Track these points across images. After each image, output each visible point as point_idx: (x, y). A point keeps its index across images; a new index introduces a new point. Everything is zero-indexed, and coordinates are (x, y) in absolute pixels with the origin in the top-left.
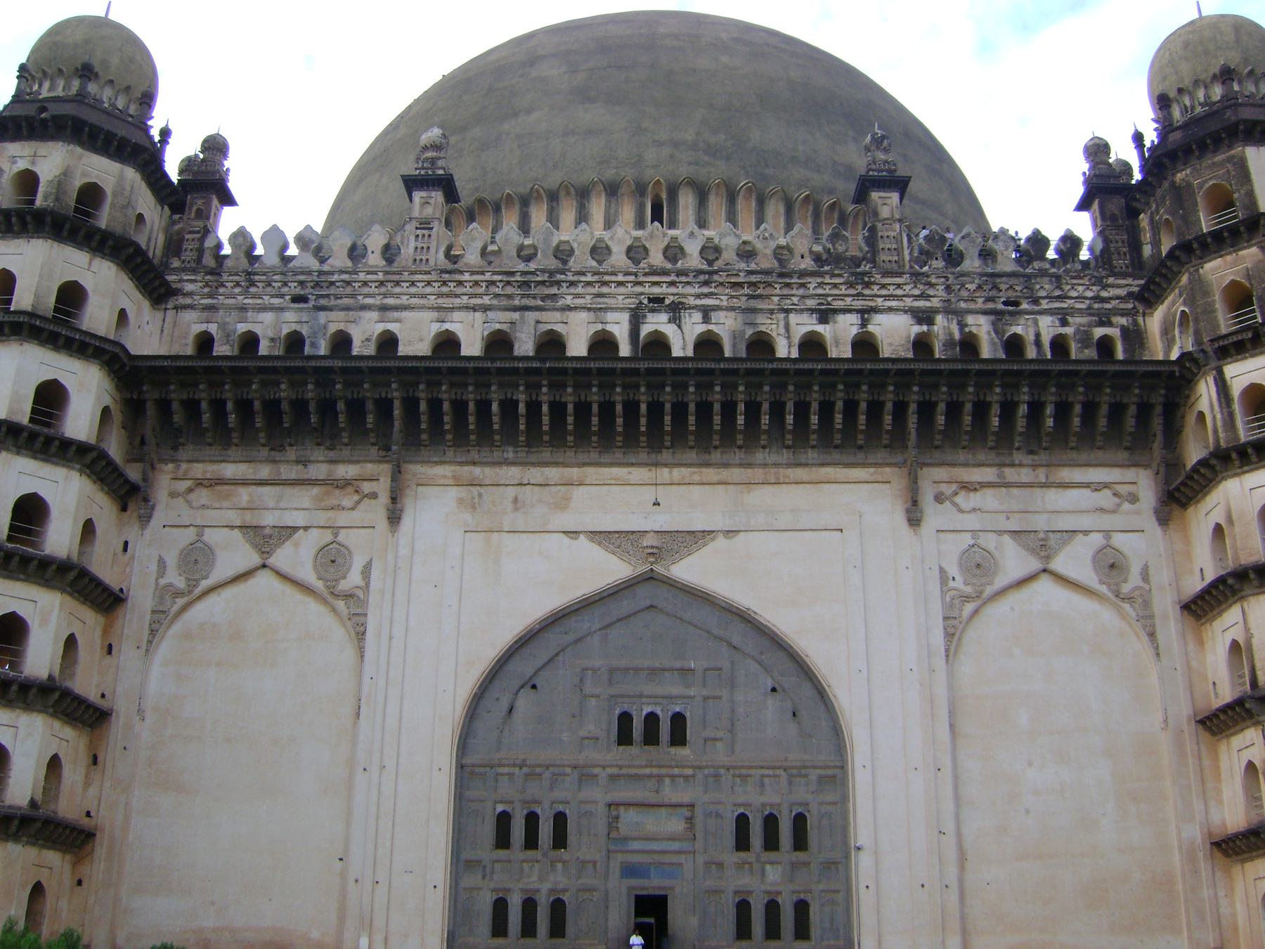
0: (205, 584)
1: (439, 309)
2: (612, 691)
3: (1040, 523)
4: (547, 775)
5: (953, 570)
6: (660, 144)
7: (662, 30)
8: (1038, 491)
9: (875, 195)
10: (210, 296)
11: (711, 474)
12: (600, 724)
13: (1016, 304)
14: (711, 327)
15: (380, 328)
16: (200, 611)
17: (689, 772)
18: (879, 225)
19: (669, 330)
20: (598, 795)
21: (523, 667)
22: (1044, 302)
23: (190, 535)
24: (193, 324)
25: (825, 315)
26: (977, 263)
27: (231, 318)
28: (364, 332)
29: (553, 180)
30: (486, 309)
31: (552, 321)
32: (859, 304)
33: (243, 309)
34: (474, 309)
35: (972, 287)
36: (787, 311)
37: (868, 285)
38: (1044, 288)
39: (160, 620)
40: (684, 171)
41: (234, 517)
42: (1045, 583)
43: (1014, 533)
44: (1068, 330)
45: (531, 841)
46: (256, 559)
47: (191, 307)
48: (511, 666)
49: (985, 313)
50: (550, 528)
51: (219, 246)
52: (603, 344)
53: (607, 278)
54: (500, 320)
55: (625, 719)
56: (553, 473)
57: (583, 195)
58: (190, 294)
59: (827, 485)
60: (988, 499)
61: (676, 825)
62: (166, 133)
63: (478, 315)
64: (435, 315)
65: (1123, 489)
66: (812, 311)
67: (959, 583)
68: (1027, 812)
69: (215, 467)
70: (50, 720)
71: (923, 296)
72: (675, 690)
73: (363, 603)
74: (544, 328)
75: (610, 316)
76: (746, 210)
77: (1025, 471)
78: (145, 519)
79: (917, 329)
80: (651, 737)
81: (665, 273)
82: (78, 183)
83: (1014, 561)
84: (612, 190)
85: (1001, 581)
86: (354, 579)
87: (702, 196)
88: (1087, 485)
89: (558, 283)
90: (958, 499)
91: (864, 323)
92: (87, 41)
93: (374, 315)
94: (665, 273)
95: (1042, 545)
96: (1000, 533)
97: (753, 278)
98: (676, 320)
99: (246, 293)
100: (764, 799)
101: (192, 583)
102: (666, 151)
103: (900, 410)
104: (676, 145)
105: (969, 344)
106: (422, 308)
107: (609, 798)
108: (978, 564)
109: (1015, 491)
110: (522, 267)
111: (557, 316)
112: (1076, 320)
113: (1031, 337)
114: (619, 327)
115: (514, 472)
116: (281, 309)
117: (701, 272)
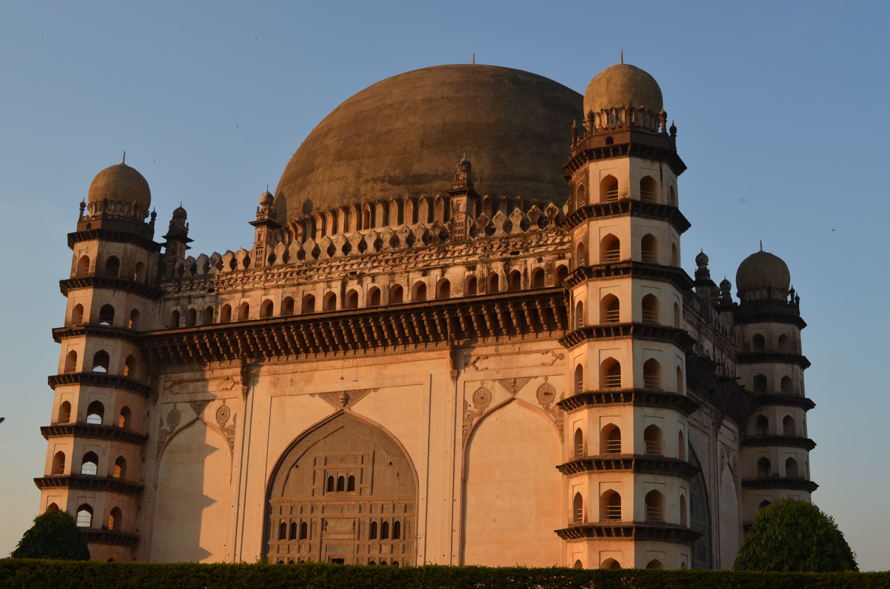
0: (177, 428)
1: (265, 289)
2: (326, 467)
3: (513, 374)
4: (299, 507)
5: (470, 401)
6: (367, 181)
7: (388, 102)
8: (515, 356)
9: (455, 200)
10: (178, 292)
11: (369, 360)
12: (320, 483)
13: (518, 253)
14: (376, 285)
15: (243, 300)
16: (177, 440)
17: (354, 503)
18: (456, 217)
19: (357, 288)
20: (318, 515)
21: (292, 458)
22: (531, 250)
23: (171, 406)
24: (172, 307)
25: (425, 272)
26: (502, 231)
27: (184, 302)
28: (235, 302)
29: (324, 207)
30: (283, 286)
31: (309, 289)
32: (442, 263)
33: (189, 298)
34: (278, 287)
35: (496, 246)
36: (408, 272)
37: (447, 252)
38: (534, 240)
39: (163, 445)
40: (379, 195)
41: (187, 397)
42: (513, 405)
43: (501, 381)
44: (543, 265)
45: (293, 536)
46: (195, 416)
47: (170, 299)
48: (287, 458)
49: (500, 260)
50: (304, 392)
51: (182, 266)
52: (331, 298)
53: (333, 264)
54: (289, 292)
55: (331, 479)
56: (306, 366)
57: (335, 214)
58: (170, 293)
59: (417, 362)
60: (490, 363)
61: (349, 527)
62: (154, 215)
63: (280, 290)
64: (263, 292)
65: (558, 352)
66: (419, 270)
67: (472, 408)
68: (495, 520)
69: (178, 375)
70: (110, 494)
71: (474, 254)
72: (350, 466)
73: (233, 432)
74: (306, 293)
75: (334, 284)
76: (409, 209)
77: (509, 346)
78: (155, 401)
79: (468, 273)
80: (340, 488)
81: (356, 257)
82: (105, 258)
83: (499, 395)
84: (346, 210)
85: (492, 405)
86: (230, 422)
87: (386, 206)
88: (538, 352)
89: (313, 269)
90: (477, 364)
91: (443, 275)
92: (107, 185)
93: (239, 295)
94: (356, 257)
95: (513, 385)
96: (494, 380)
97: (395, 256)
98: (360, 283)
99: (191, 289)
100: (383, 515)
101: (173, 428)
102: (371, 184)
103: (443, 322)
104: (374, 180)
105: (495, 277)
106: (258, 288)
107: (323, 516)
108: (482, 397)
109: (504, 357)
110: (299, 263)
111: (311, 286)
112: (547, 258)
113: (522, 272)
114: (336, 289)
115: (291, 366)
116: (203, 297)
117: (371, 256)
